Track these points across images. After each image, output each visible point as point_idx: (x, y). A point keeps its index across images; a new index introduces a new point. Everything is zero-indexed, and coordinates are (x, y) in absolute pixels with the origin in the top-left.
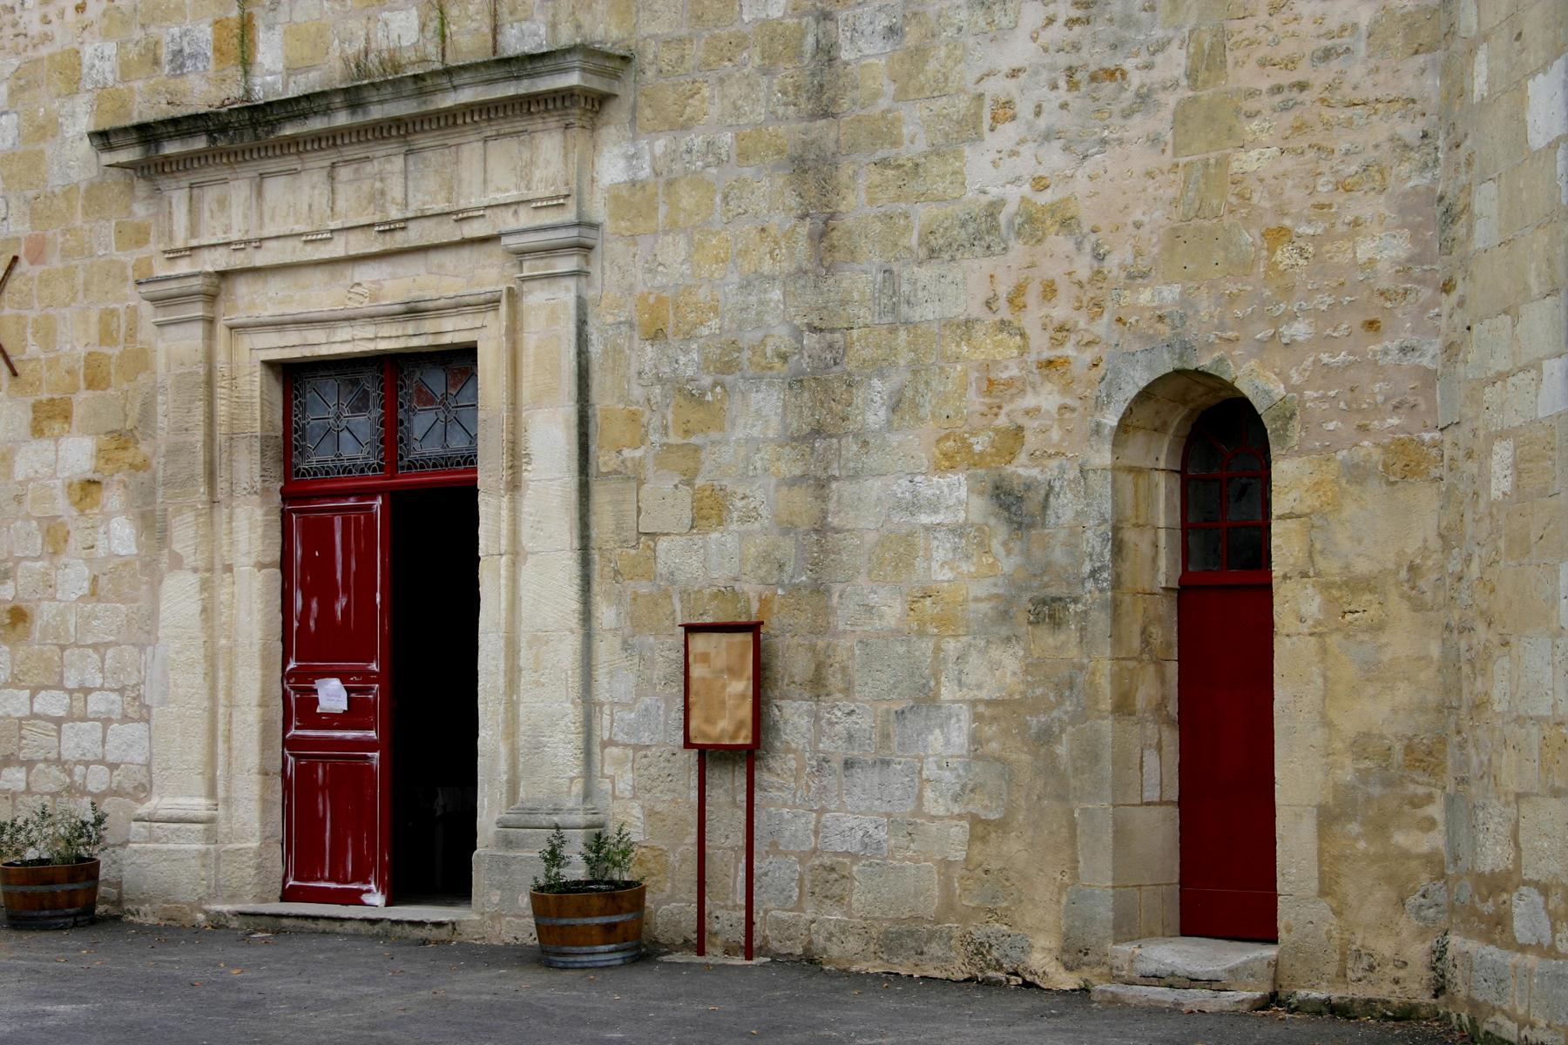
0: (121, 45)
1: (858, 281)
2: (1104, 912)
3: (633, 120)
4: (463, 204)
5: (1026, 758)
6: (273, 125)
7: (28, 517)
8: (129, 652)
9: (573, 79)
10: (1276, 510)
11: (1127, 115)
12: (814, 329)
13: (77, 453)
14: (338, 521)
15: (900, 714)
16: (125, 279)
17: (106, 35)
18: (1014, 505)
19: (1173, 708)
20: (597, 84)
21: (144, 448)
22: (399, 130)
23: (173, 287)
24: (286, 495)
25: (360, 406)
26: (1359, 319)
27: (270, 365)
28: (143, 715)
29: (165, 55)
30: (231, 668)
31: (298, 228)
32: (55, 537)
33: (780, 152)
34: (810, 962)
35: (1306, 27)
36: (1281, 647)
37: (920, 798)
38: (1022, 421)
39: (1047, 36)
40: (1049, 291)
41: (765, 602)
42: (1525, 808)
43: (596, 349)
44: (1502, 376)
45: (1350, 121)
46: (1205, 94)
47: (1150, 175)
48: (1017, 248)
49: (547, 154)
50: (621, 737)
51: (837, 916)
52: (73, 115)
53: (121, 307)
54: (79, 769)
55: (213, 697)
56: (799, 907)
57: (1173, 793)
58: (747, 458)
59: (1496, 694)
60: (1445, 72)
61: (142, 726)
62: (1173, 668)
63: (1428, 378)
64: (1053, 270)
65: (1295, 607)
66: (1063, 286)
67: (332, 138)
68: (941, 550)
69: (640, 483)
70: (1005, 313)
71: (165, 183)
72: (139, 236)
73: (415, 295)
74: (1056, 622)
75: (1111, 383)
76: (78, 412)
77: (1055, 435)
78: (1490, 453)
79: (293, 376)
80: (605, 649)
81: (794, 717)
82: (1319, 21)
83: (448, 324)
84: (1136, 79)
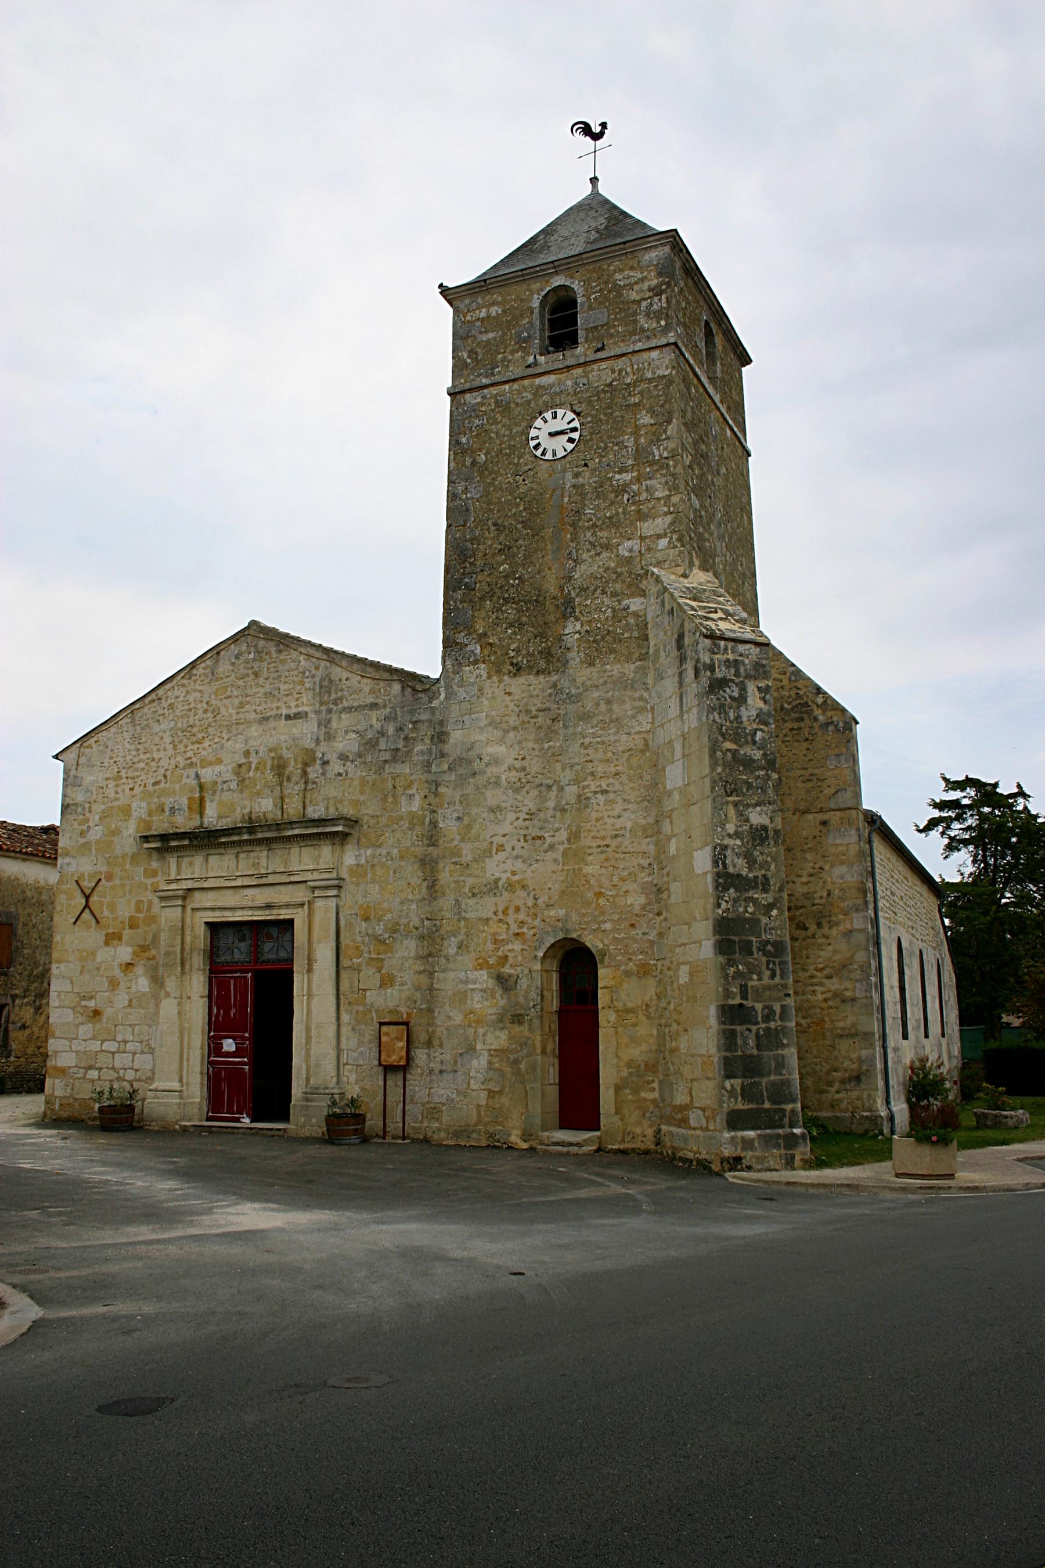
0: (149, 804)
1: (446, 903)
2: (538, 1121)
3: (358, 843)
4: (291, 869)
5: (509, 1069)
6: (217, 838)
7: (102, 976)
8: (145, 1028)
9: (340, 828)
10: (600, 985)
11: (546, 852)
12: (428, 919)
13: (125, 952)
14: (232, 981)
15: (461, 1054)
16: (147, 889)
17: (142, 799)
18: (505, 982)
19: (557, 1052)
20: (347, 830)
21: (153, 952)
22: (267, 842)
23: (170, 893)
24: (211, 971)
25: (242, 939)
26: (627, 923)
27: (206, 923)
28: (152, 1051)
29: (167, 809)
30: (190, 1035)
31: (223, 874)
32: (114, 984)
33: (416, 857)
34: (426, 1141)
35: (609, 827)
36: (602, 1032)
37: (469, 1083)
38: (507, 953)
39: (516, 824)
40: (517, 909)
41: (409, 1014)
42: (694, 1083)
43: (342, 923)
44: (685, 945)
45: (624, 859)
46: (574, 846)
47: (554, 872)
48: (505, 894)
49: (326, 852)
50: (351, 1062)
51: (436, 1125)
52: (127, 828)
53: (145, 900)
54: (122, 1071)
55: (182, 1045)
56: (422, 1122)
57: (557, 1081)
58: (402, 964)
59: (681, 1047)
60: (656, 844)
61: (150, 1056)
62: (557, 1038)
63: (652, 943)
64: (519, 903)
65: (606, 1018)
66: (522, 908)
67: (240, 843)
68: (477, 997)
69: (360, 971)
70: (501, 916)
71: (167, 855)
72: (154, 874)
73: (269, 900)
74: (520, 1023)
75: (541, 942)
76: (125, 937)
77: (520, 958)
78: (678, 969)
79: (214, 927)
80: (344, 1030)
81: (420, 1055)
82: (613, 825)
83: (282, 911)
84: (549, 840)
